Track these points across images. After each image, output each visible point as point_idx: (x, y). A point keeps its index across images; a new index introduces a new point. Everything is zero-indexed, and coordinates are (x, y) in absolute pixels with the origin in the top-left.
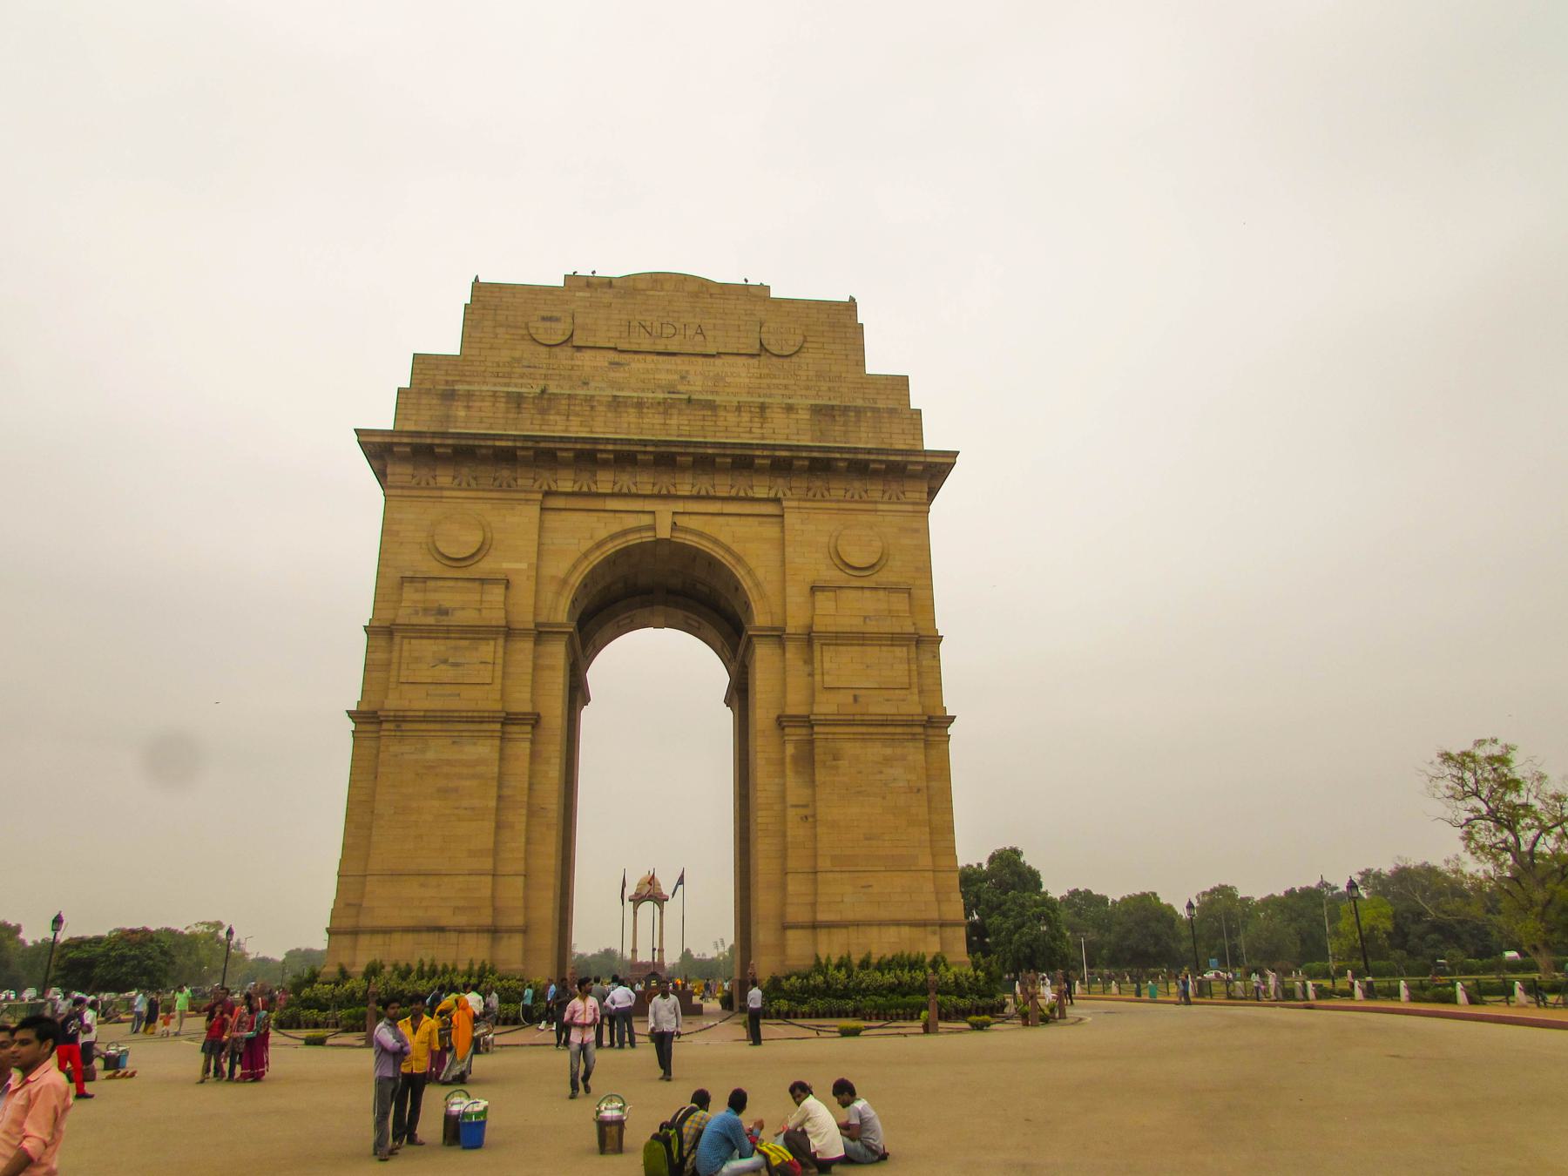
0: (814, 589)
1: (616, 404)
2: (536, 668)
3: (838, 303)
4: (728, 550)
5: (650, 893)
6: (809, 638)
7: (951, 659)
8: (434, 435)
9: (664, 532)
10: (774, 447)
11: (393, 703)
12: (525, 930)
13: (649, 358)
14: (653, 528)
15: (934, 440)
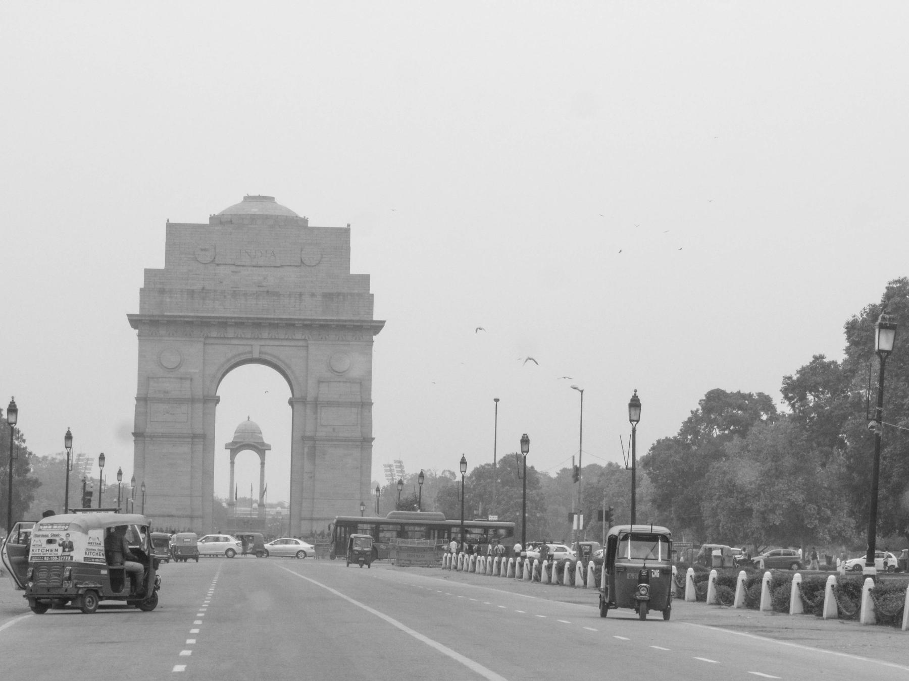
0: (320, 382)
1: (235, 294)
2: (204, 414)
3: (341, 229)
4: (283, 362)
5: (249, 441)
6: (316, 404)
7: (376, 412)
8: (159, 316)
9: (256, 355)
10: (305, 320)
11: (149, 430)
12: (202, 517)
13: (250, 269)
14: (251, 352)
15: (377, 315)
